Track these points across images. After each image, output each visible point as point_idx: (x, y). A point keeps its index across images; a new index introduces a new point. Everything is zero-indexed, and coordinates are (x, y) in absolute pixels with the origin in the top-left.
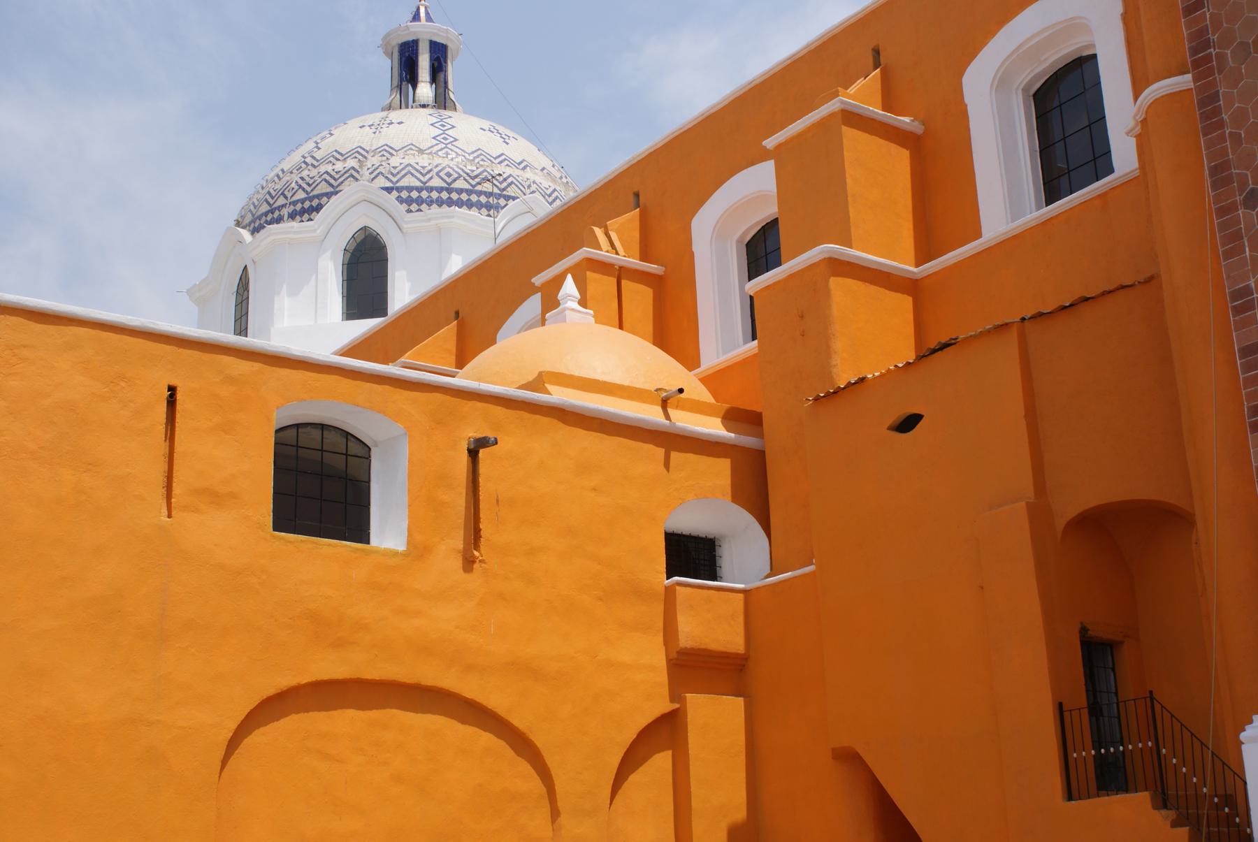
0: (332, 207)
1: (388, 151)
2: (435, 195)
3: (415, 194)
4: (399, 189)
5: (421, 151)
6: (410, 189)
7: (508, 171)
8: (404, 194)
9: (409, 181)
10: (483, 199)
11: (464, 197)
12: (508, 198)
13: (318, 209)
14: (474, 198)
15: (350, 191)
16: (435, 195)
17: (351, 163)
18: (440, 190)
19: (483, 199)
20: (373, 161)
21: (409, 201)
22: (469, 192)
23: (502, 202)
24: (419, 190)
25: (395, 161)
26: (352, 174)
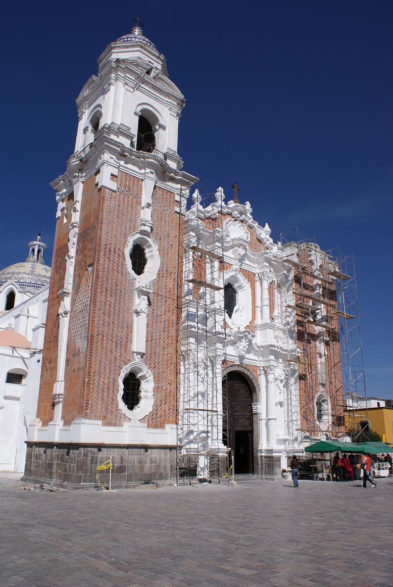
0: (5, 284)
1: (19, 273)
2: (27, 284)
3: (23, 284)
4: (19, 282)
5: (26, 274)
6: (22, 282)
7: (45, 279)
8: (20, 283)
9: (22, 281)
10: (38, 285)
11: (33, 285)
12: (43, 285)
13: (2, 285)
14: (36, 285)
15: (9, 281)
16: (27, 284)
17: (11, 275)
18: (28, 283)
19: (38, 285)
20: (15, 275)
21: (21, 285)
22: (35, 284)
23: (42, 286)
24: (24, 283)
25: (20, 276)
26: (10, 278)
